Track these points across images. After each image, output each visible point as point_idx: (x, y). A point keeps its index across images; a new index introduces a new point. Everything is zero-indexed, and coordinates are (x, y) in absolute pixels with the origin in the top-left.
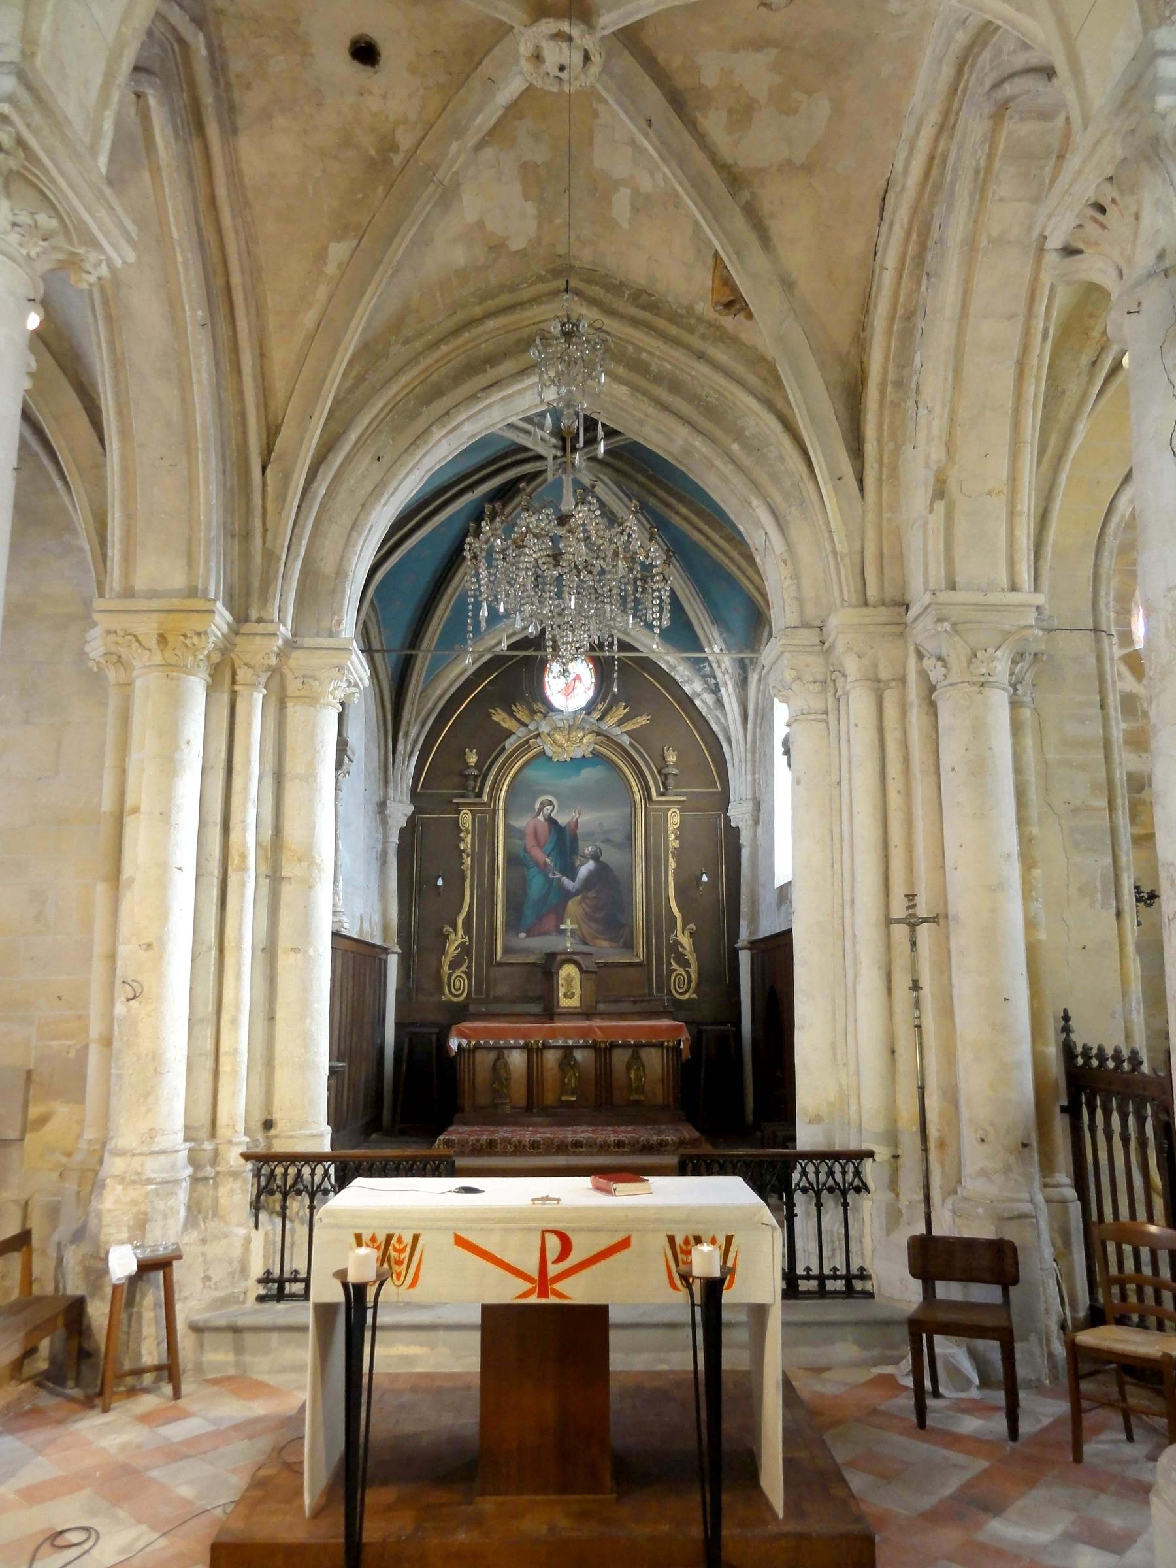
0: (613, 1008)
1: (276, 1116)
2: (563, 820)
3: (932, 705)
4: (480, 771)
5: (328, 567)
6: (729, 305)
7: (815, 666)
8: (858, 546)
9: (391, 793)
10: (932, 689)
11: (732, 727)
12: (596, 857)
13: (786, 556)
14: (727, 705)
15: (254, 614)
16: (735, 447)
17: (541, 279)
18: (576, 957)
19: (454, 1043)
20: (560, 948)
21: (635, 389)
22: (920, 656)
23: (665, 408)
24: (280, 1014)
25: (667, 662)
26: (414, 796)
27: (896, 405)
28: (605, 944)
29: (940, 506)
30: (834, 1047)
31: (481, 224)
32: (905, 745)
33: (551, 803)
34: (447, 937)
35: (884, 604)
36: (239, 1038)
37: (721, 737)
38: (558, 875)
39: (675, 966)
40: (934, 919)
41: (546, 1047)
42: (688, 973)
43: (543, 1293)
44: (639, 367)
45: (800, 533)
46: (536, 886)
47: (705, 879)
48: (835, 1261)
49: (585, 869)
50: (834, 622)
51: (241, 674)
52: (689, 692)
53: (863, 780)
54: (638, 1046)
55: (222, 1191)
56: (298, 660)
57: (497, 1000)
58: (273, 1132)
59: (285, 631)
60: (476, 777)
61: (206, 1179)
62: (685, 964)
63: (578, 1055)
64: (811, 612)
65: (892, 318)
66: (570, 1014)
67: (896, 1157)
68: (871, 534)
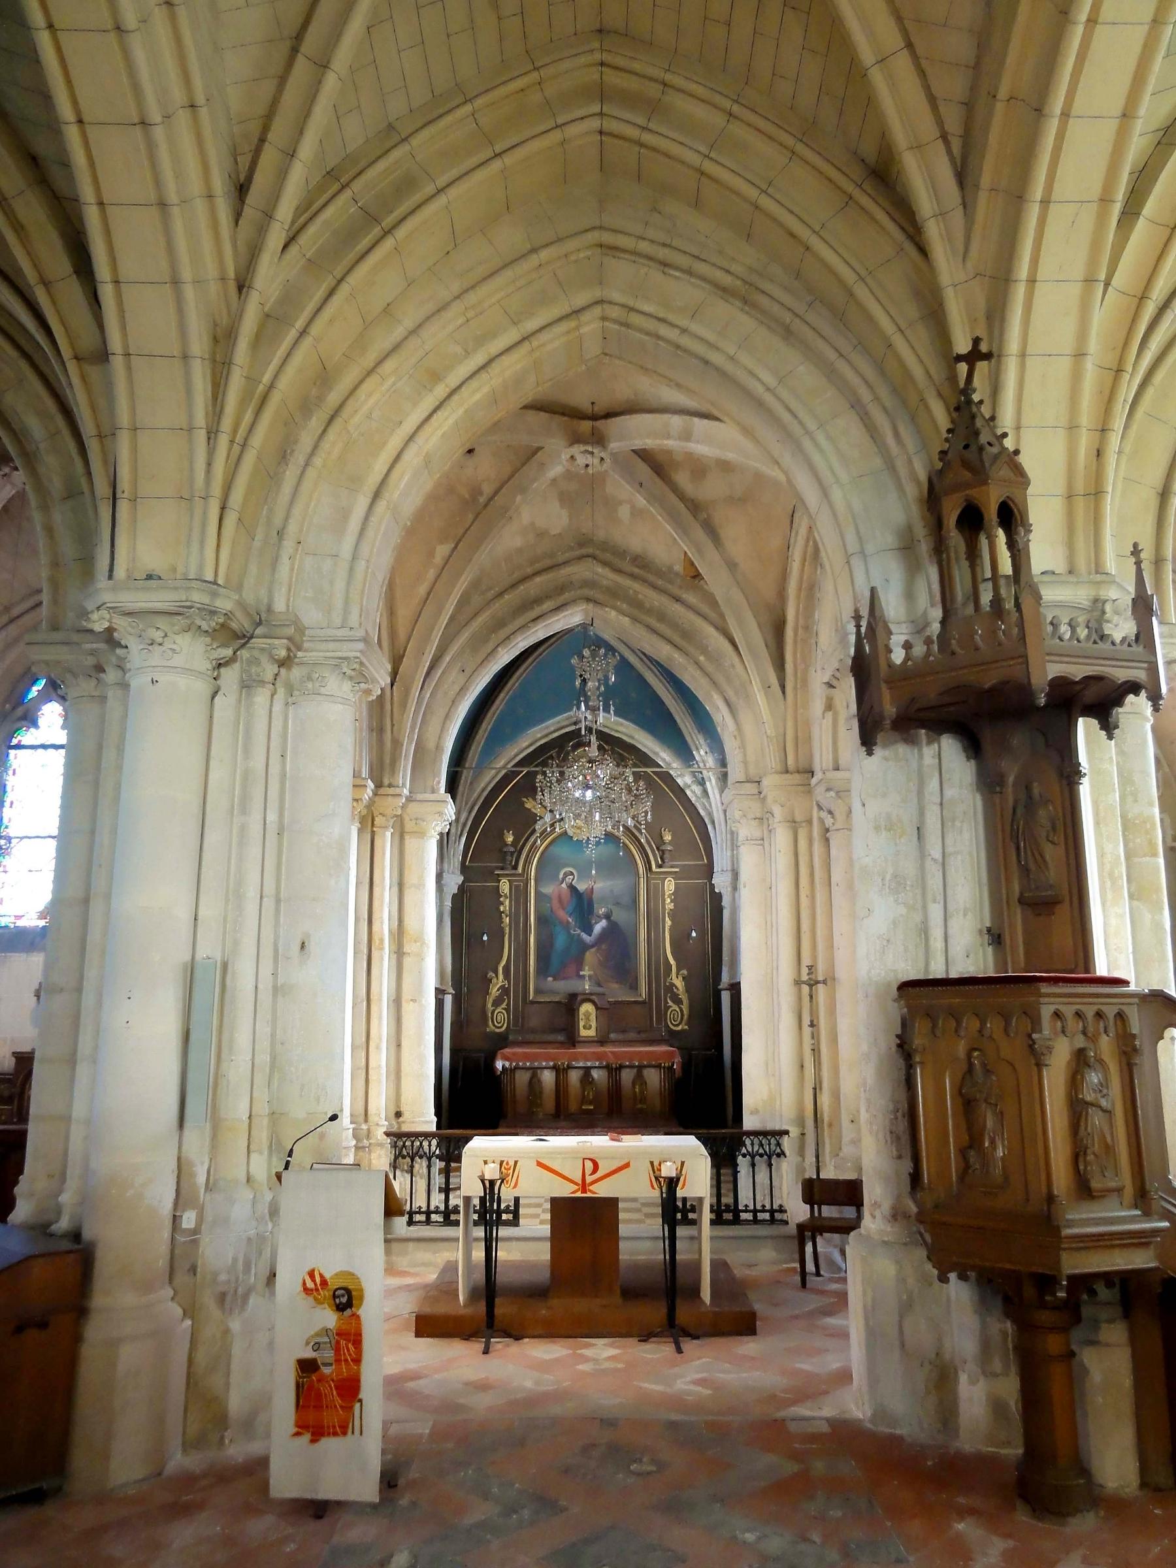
0: (621, 1037)
1: (404, 1108)
2: (582, 887)
3: (827, 840)
4: (515, 847)
5: (431, 745)
6: (694, 577)
7: (755, 809)
8: (781, 730)
9: (446, 866)
10: (827, 830)
11: (715, 814)
12: (608, 917)
13: (736, 733)
14: (711, 796)
15: (386, 782)
16: (702, 658)
17: (572, 549)
18: (593, 997)
19: (499, 1065)
20: (580, 989)
21: (635, 620)
22: (820, 808)
23: (654, 631)
24: (404, 1043)
25: (664, 760)
26: (464, 869)
28: (616, 986)
29: (829, 715)
30: (767, 1065)
31: (533, 524)
32: (812, 868)
33: (572, 874)
34: (490, 981)
35: (798, 772)
36: (381, 1058)
37: (707, 821)
38: (579, 931)
39: (670, 1003)
40: (824, 982)
41: (570, 1067)
42: (681, 1010)
43: (584, 1191)
44: (637, 604)
45: (745, 717)
46: (560, 941)
47: (694, 934)
48: (763, 1200)
49: (599, 927)
50: (766, 782)
51: (378, 821)
52: (681, 784)
53: (784, 889)
54: (640, 1068)
55: (373, 1156)
56: (413, 808)
57: (533, 1031)
58: (401, 1119)
59: (406, 792)
60: (512, 853)
61: (364, 1147)
62: (678, 1002)
63: (595, 1074)
64: (752, 771)
65: (800, 589)
66: (588, 1042)
67: (803, 1134)
68: (790, 724)
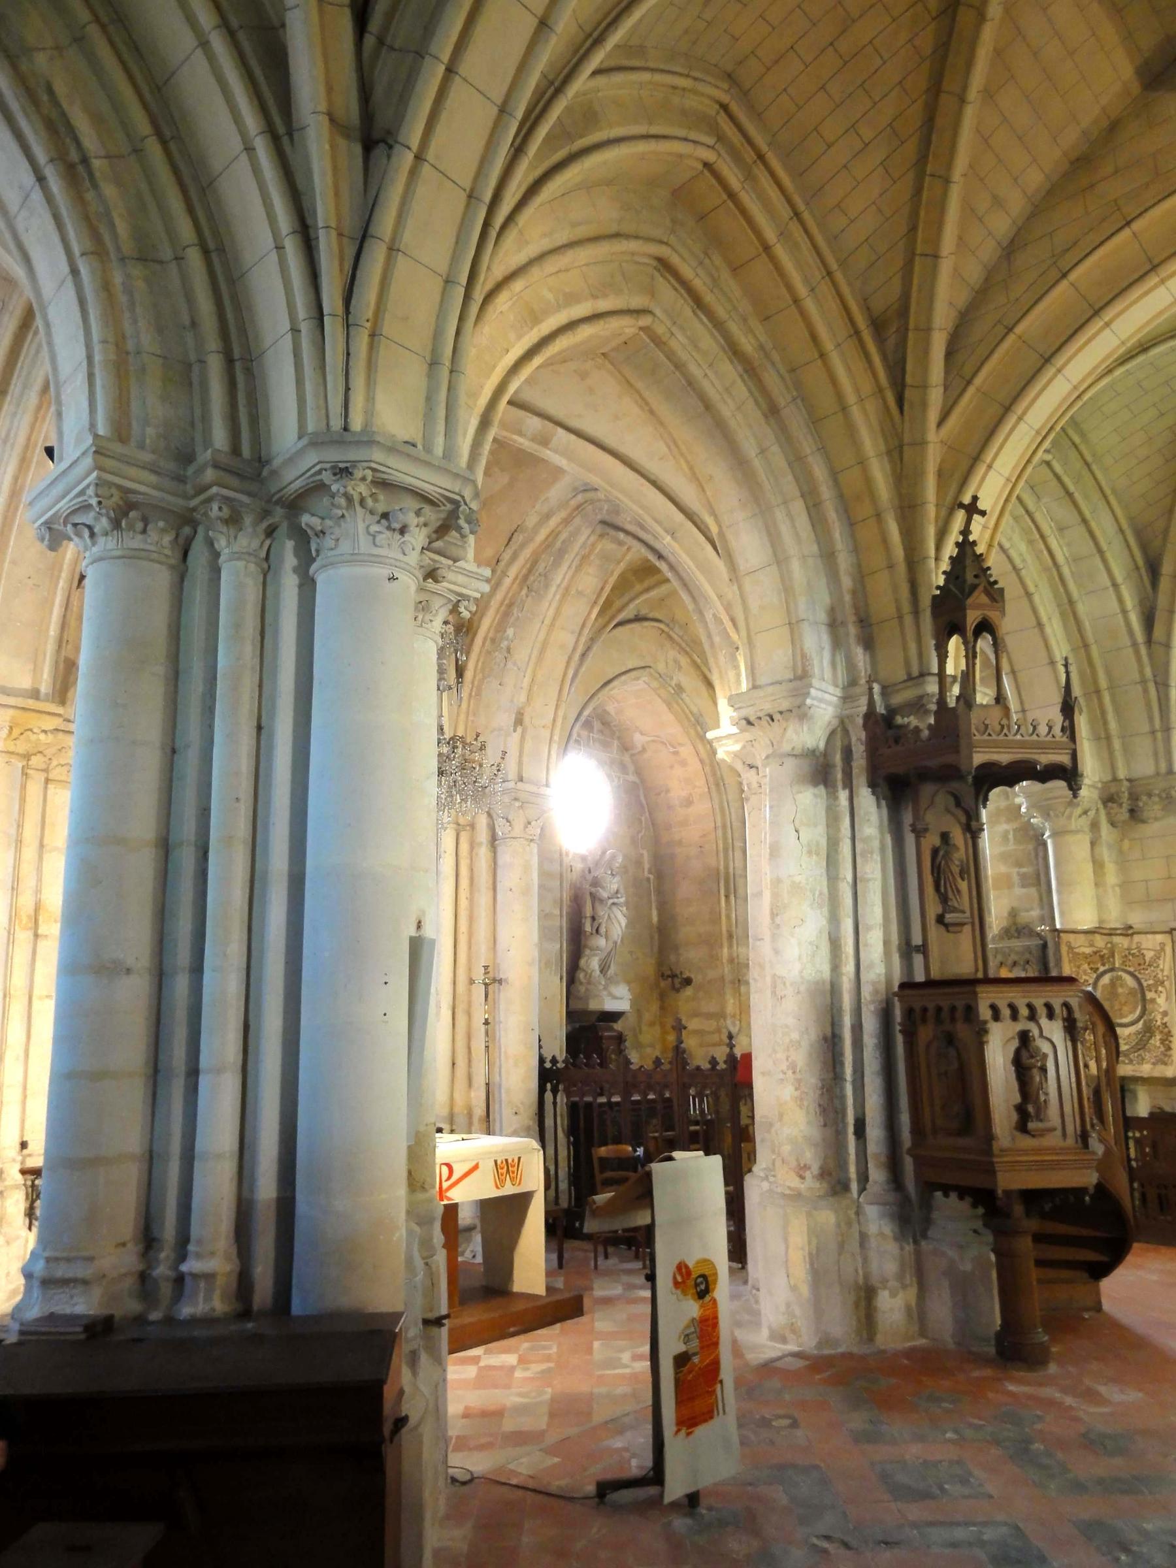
27: (489, 653)
58: (25, 1152)
65: (502, 604)
